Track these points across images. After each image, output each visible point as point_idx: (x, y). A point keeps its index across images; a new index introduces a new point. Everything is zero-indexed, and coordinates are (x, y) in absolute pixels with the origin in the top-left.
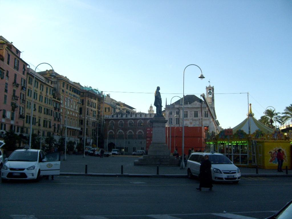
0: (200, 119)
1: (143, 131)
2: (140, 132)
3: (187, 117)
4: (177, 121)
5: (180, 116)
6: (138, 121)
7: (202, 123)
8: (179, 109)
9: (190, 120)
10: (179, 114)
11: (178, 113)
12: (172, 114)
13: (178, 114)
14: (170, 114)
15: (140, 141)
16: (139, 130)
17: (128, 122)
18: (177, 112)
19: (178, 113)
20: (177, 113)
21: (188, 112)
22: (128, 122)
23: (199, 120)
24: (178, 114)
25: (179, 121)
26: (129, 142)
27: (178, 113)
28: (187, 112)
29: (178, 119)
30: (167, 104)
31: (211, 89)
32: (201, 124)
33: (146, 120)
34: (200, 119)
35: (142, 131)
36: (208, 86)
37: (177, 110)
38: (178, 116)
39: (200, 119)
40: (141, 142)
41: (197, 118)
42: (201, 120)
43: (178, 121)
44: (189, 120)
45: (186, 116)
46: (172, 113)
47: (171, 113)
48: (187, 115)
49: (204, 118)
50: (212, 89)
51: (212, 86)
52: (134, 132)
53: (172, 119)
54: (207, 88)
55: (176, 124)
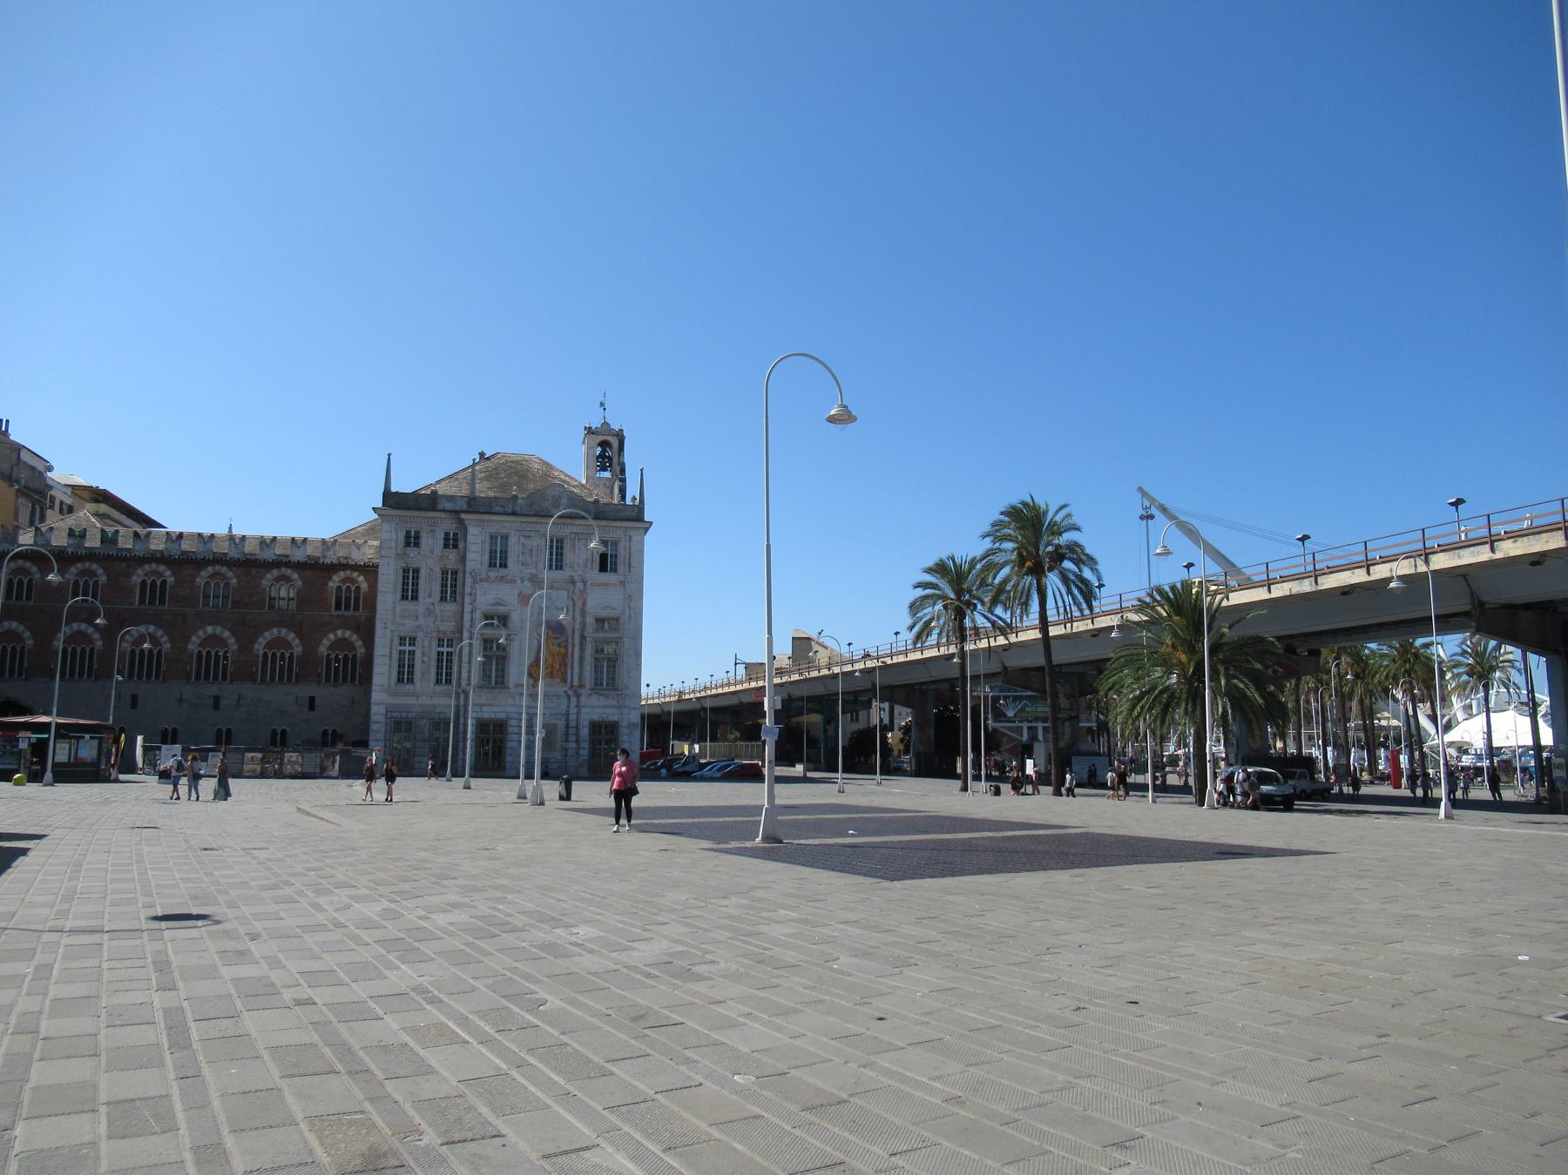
0: (573, 582)
1: (233, 632)
2: (214, 640)
3: (504, 565)
4: (444, 585)
5: (463, 560)
6: (203, 573)
7: (584, 604)
8: (461, 522)
9: (522, 581)
10: (461, 545)
11: (456, 540)
12: (417, 544)
13: (456, 546)
14: (407, 544)
15: (213, 690)
16: (210, 629)
17: (137, 579)
18: (447, 534)
19: (452, 542)
20: (446, 539)
21: (513, 540)
22: (137, 579)
23: (571, 588)
24: (456, 546)
25: (459, 582)
26: (134, 699)
27: (452, 542)
28: (505, 538)
29: (455, 573)
30: (393, 489)
31: (609, 438)
32: (579, 604)
33: (254, 571)
34: (577, 578)
35: (226, 634)
36: (596, 423)
37: (449, 526)
38: (452, 555)
39: (573, 582)
40: (217, 699)
41: (561, 572)
42: (579, 585)
43: (454, 586)
44: (513, 581)
45: (498, 559)
46: (417, 537)
47: (412, 540)
48: (504, 553)
49: (595, 575)
50: (615, 442)
51: (615, 426)
52: (169, 634)
53: (416, 571)
54: (589, 431)
55: (443, 599)
